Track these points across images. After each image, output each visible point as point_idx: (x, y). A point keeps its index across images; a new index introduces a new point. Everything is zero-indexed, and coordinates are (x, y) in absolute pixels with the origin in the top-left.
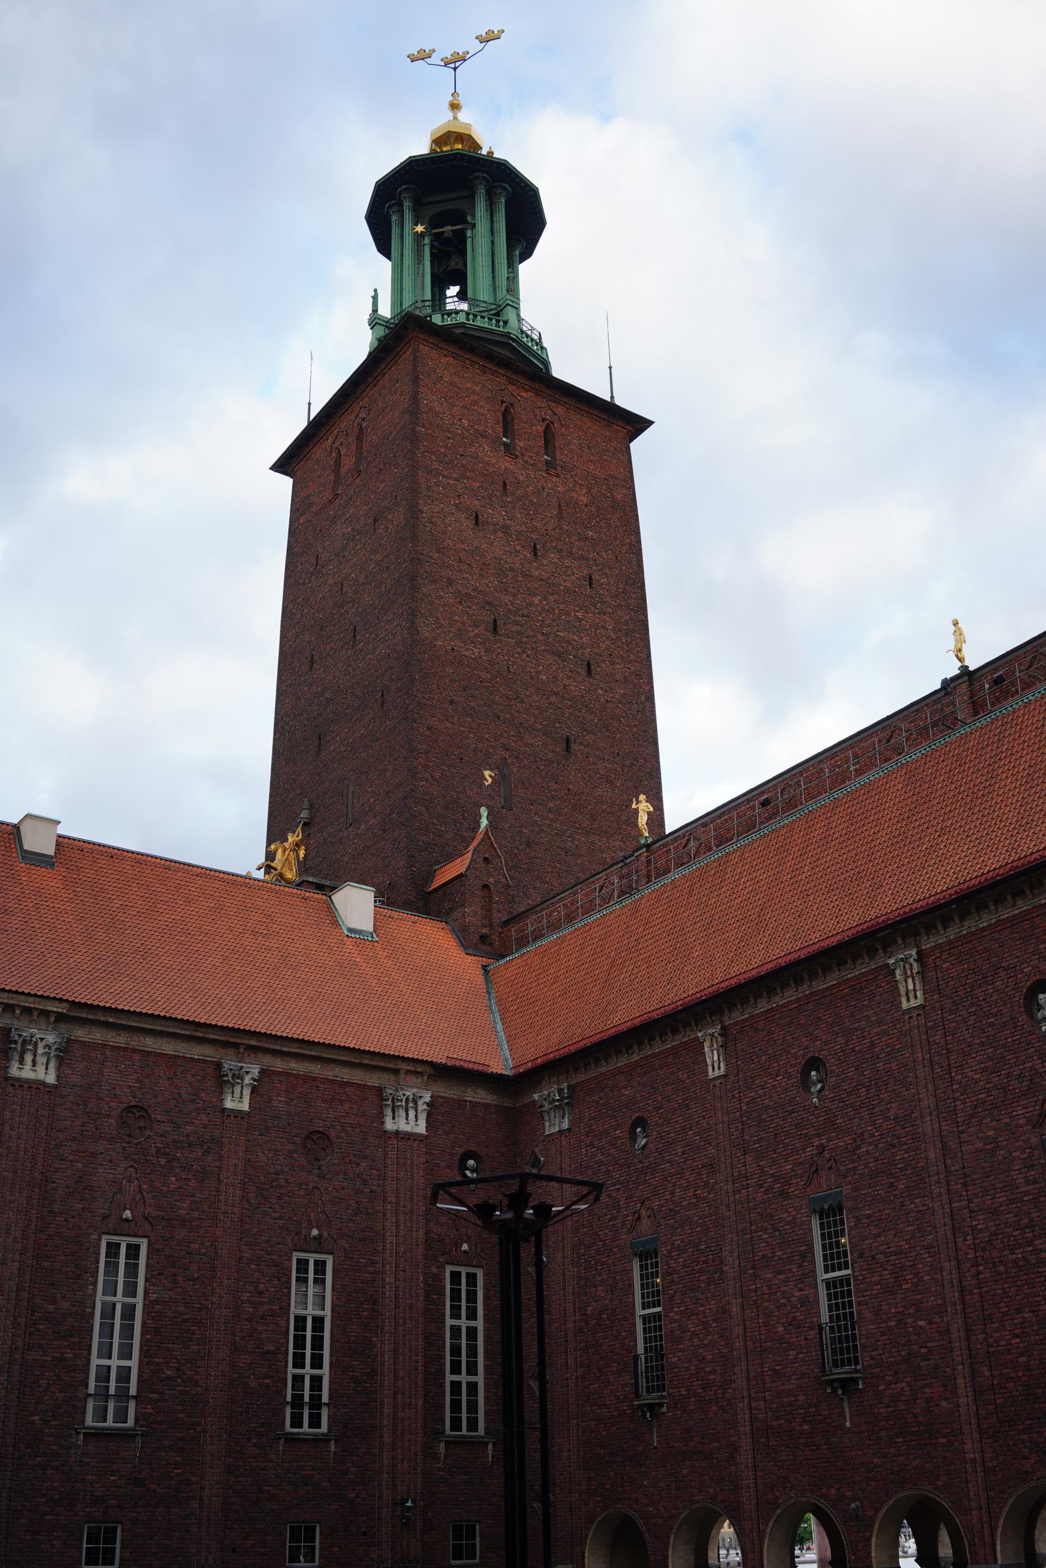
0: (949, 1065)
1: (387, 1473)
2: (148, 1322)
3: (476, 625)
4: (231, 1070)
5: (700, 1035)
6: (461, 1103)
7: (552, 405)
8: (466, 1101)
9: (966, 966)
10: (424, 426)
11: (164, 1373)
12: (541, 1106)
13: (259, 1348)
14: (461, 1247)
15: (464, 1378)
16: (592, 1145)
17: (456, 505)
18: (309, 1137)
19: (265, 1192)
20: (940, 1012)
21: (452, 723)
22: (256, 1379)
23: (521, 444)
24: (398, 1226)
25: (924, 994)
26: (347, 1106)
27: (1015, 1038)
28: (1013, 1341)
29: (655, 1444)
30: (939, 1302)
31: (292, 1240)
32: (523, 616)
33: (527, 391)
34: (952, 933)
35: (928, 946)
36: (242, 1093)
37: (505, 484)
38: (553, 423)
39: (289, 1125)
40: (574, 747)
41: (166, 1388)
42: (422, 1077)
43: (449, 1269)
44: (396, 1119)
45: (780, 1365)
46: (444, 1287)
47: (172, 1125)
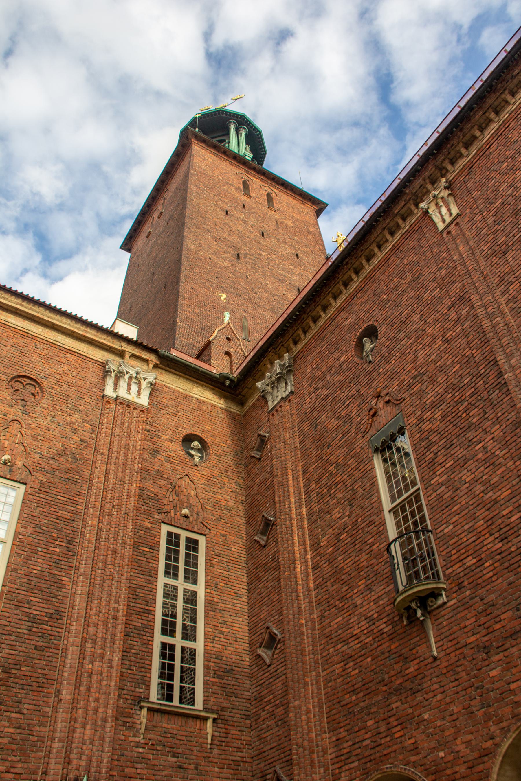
6: (187, 397)
8: (192, 397)
24: (107, 474)
42: (148, 365)
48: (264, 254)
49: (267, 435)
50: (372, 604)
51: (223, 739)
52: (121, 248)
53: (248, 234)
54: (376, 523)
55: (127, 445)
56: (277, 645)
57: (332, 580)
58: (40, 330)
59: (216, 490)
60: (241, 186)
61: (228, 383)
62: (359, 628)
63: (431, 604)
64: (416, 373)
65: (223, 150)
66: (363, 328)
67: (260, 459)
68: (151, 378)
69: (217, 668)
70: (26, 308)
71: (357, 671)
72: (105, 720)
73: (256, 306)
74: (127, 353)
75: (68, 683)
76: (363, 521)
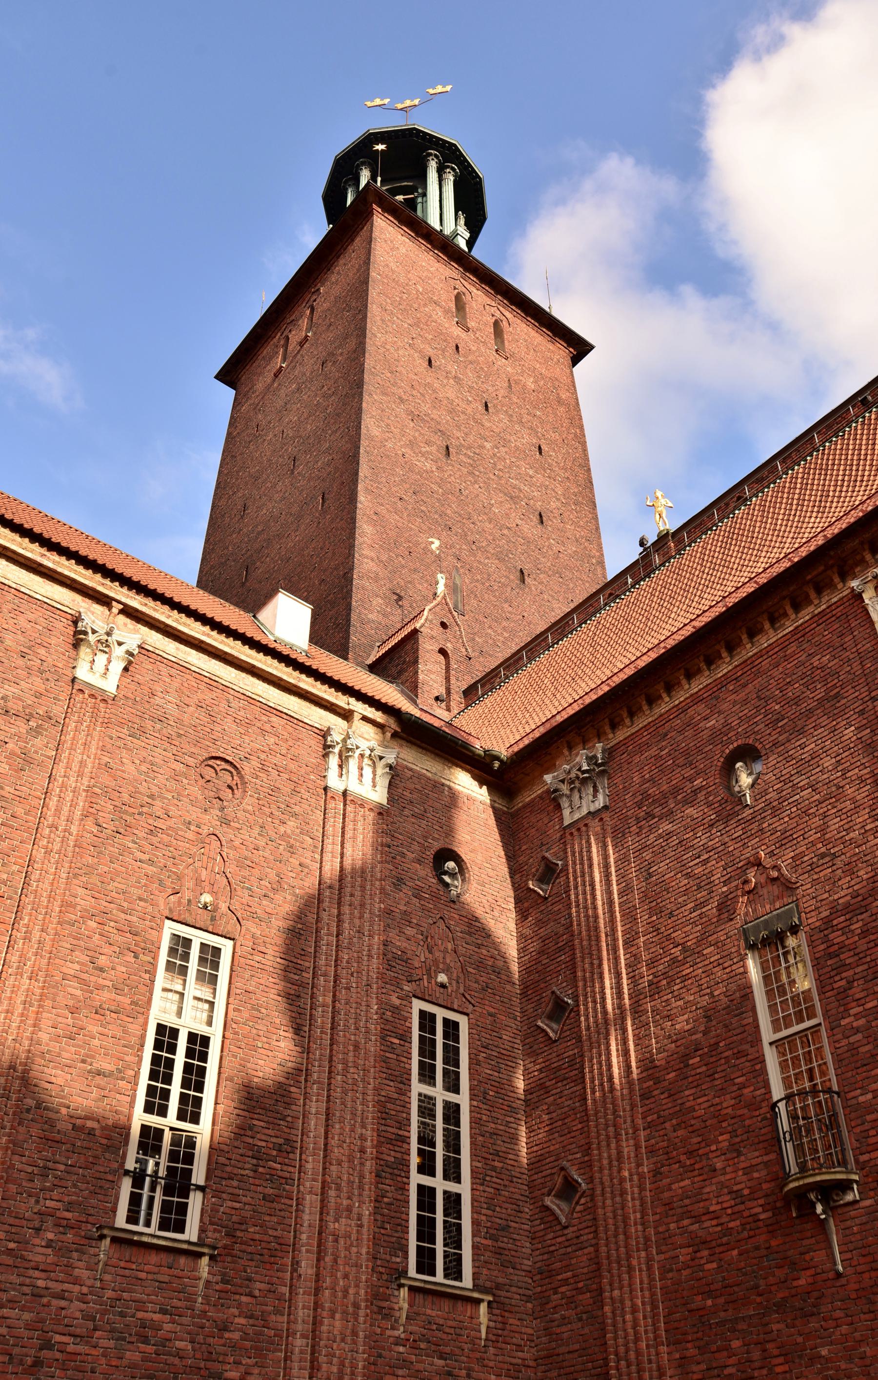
1: (303, 1336)
5: (854, 584)
8: (443, 785)
12: (556, 791)
13: (83, 1061)
15: (439, 1183)
19: (128, 818)
24: (340, 921)
29: (840, 1268)
32: (475, 453)
37: (457, 347)
39: (179, 735)
42: (384, 733)
44: (344, 777)
48: (488, 445)
49: (560, 863)
50: (740, 1173)
51: (500, 1332)
52: (216, 377)
53: (463, 405)
54: (750, 1057)
56: (580, 1198)
57: (674, 1122)
59: (479, 942)
60: (453, 305)
61: (497, 764)
62: (718, 1203)
63: (835, 1198)
64: (823, 850)
65: (425, 231)
66: (735, 745)
67: (546, 899)
68: (391, 758)
69: (489, 1224)
70: (215, 640)
71: (714, 1265)
73: (474, 547)
74: (355, 714)
75: (307, 1251)
76: (728, 1047)
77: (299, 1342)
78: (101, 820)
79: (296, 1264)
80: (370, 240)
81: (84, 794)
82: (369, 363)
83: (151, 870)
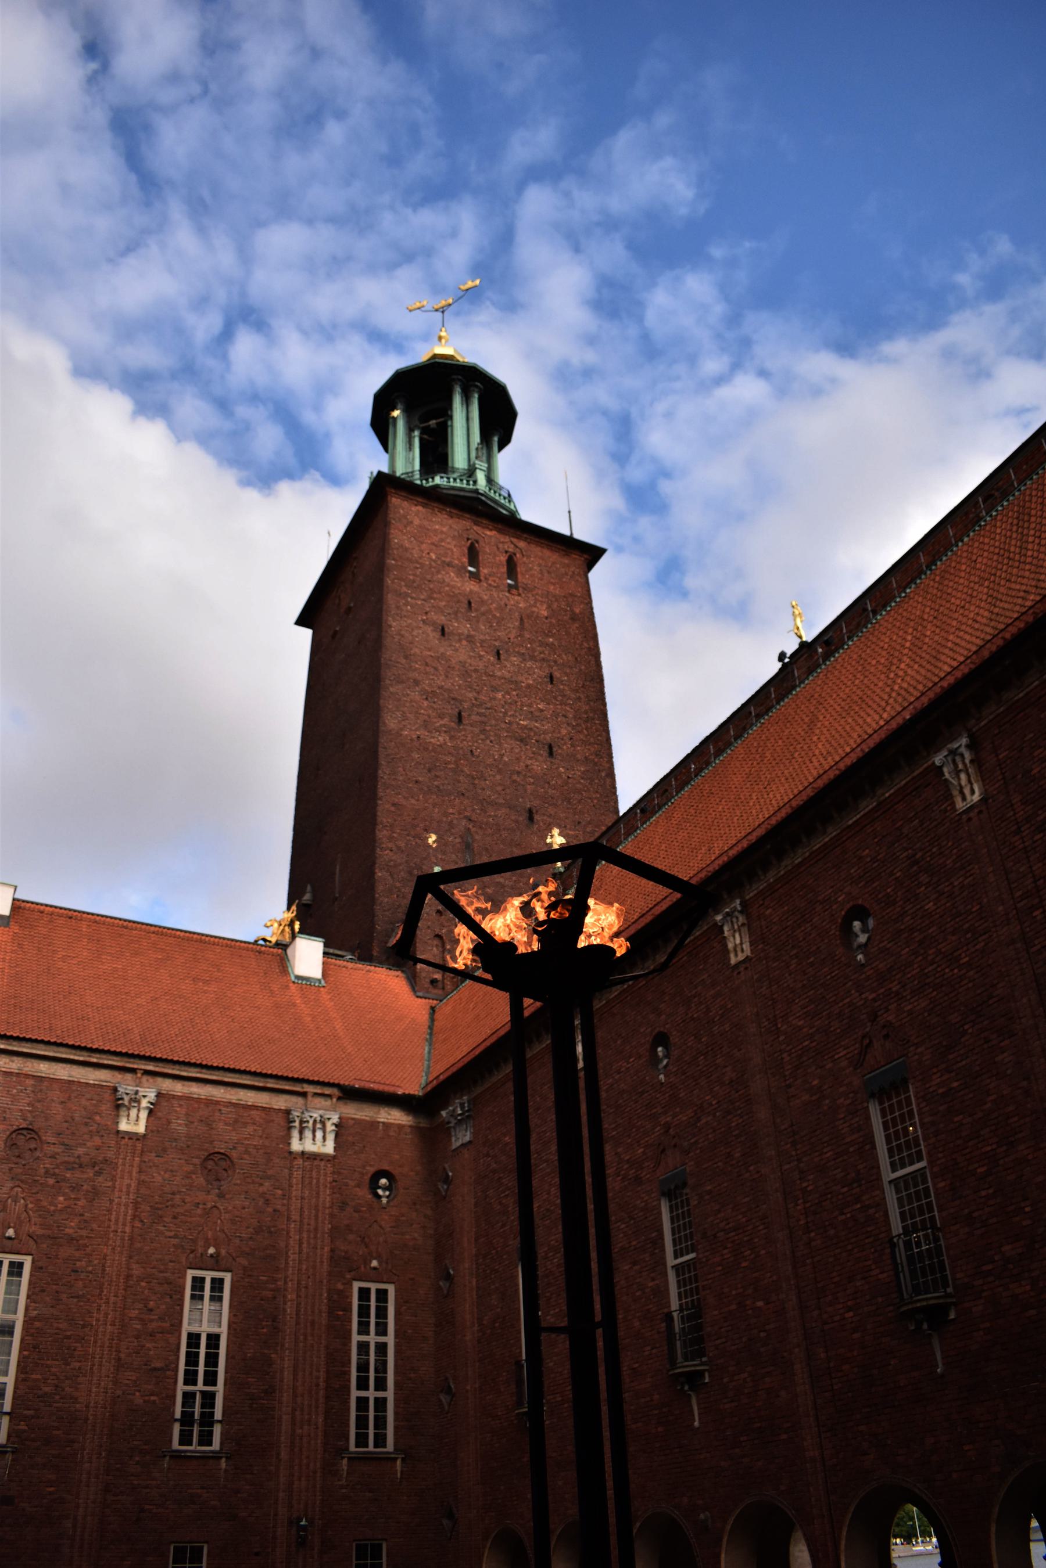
0: (775, 1016)
2: (27, 1338)
3: (441, 716)
4: (127, 1094)
6: (373, 1125)
7: (514, 540)
8: (379, 1122)
9: (786, 908)
10: (394, 560)
11: (41, 1389)
13: (146, 1365)
14: (371, 1262)
16: (488, 1155)
17: (423, 621)
18: (207, 1159)
20: (764, 962)
21: (418, 800)
22: (142, 1396)
23: (486, 571)
24: (301, 1244)
25: (751, 946)
26: (250, 1129)
27: (833, 974)
28: (847, 1315)
30: (775, 1278)
31: (187, 1258)
32: (487, 708)
33: (491, 530)
34: (771, 876)
35: (751, 895)
36: (138, 1116)
37: (470, 603)
38: (515, 554)
40: (536, 817)
41: (42, 1404)
42: (331, 1099)
43: (356, 1285)
45: (637, 1362)
46: (350, 1303)
47: (63, 1147)
48: (499, 695)
55: (317, 1206)
58: (222, 1091)
72: (315, 1472)
77: (281, 1494)
78: (143, 1218)
79: (278, 1454)
80: (387, 524)
81: (131, 1205)
82: (386, 656)
83: (175, 1241)
